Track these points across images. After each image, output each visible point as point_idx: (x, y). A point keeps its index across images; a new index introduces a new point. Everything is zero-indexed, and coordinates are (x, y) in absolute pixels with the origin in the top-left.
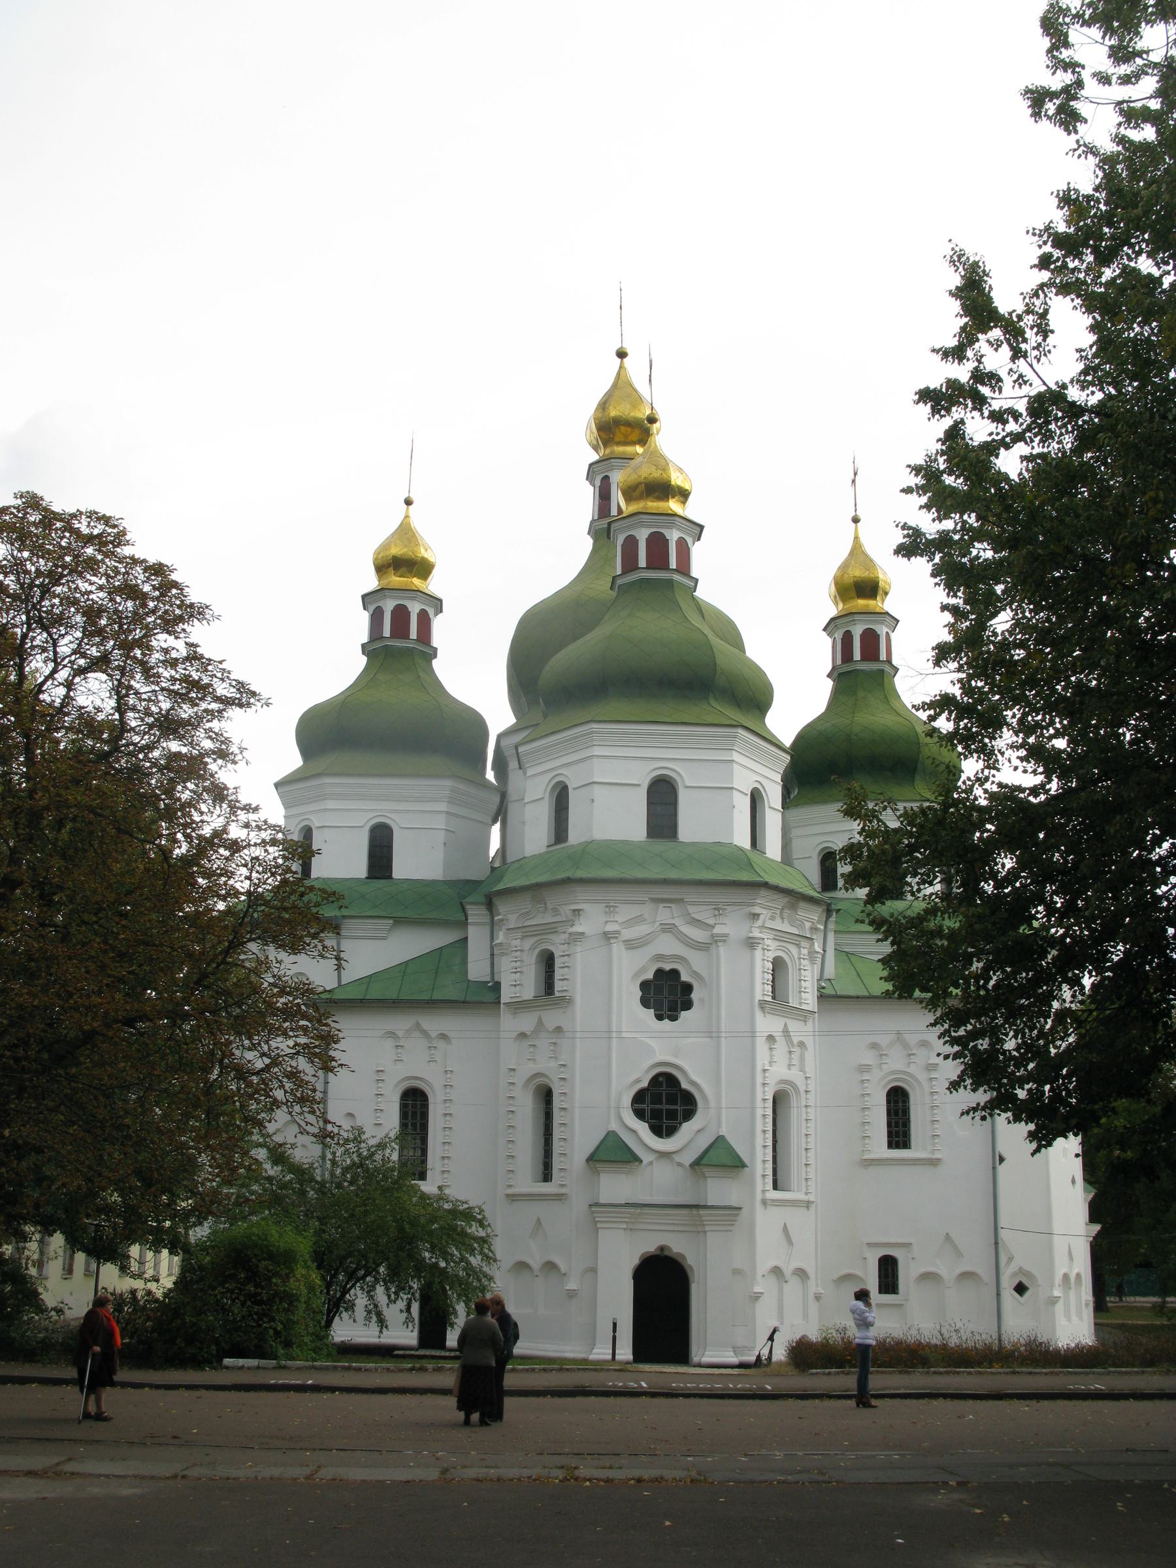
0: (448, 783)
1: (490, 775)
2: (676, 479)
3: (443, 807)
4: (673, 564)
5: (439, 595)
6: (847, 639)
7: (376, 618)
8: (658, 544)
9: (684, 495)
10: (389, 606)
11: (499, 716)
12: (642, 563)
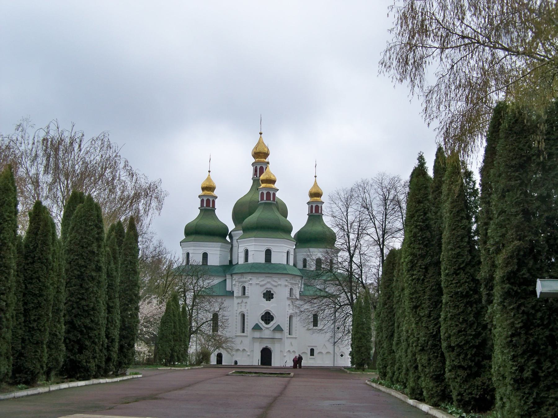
0: (220, 244)
1: (228, 238)
2: (273, 178)
3: (219, 249)
4: (272, 199)
5: (217, 195)
6: (312, 206)
7: (202, 201)
8: (268, 194)
9: (273, 182)
10: (205, 199)
11: (231, 226)
12: (265, 199)
